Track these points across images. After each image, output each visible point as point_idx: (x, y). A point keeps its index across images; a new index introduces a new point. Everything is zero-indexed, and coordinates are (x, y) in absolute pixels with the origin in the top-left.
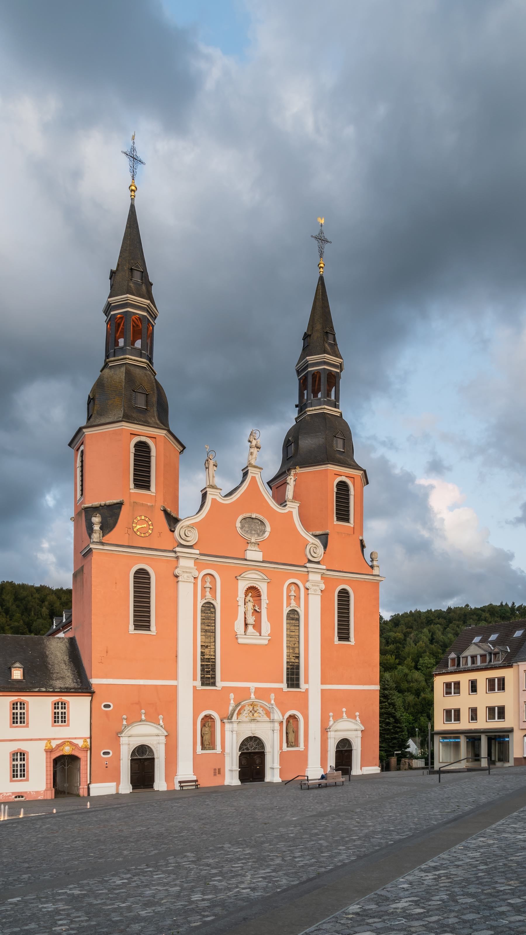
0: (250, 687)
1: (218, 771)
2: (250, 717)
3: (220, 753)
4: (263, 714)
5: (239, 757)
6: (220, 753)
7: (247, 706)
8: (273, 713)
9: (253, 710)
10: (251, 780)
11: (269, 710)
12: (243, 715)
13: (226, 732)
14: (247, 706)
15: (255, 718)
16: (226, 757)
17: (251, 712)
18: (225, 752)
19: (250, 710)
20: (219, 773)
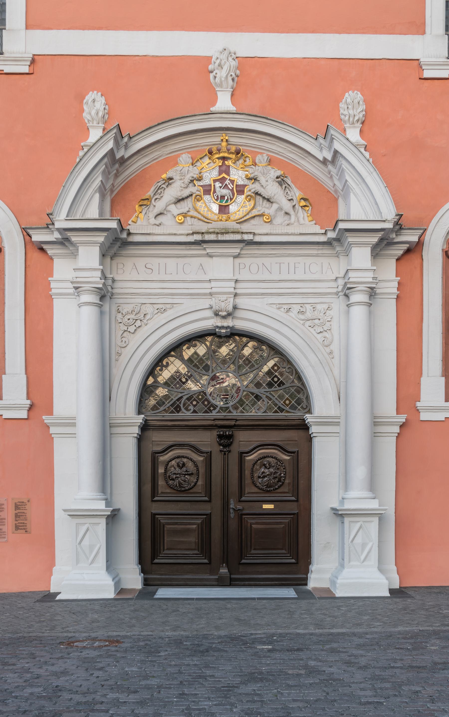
0: (208, 59)
1: (17, 516)
2: (207, 220)
3: (24, 414)
4: (287, 206)
5: (140, 440)
6: (24, 414)
7: (185, 158)
8: (346, 197)
9: (222, 180)
10: (224, 571)
11: (328, 184)
12: (159, 205)
13: (58, 304)
14: (185, 158)
15: (232, 225)
16: (56, 441)
17: (207, 190)
18: (50, 412)
19: (207, 181)
20: (17, 528)
